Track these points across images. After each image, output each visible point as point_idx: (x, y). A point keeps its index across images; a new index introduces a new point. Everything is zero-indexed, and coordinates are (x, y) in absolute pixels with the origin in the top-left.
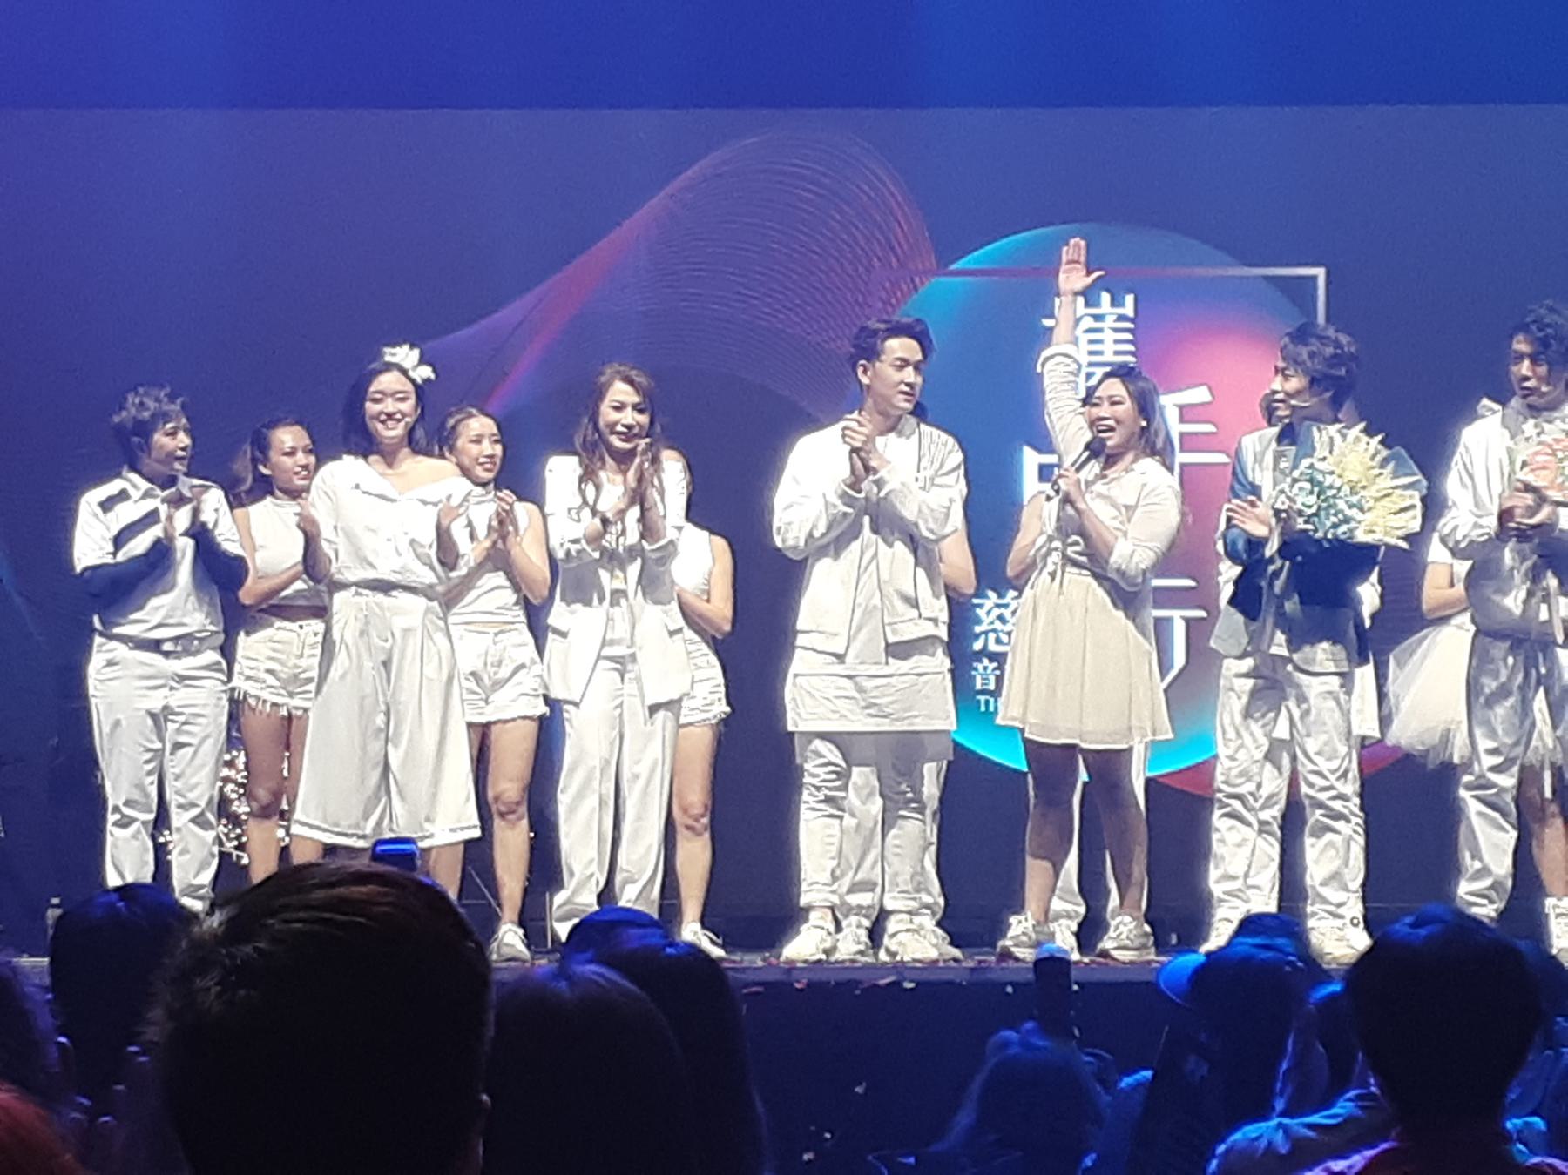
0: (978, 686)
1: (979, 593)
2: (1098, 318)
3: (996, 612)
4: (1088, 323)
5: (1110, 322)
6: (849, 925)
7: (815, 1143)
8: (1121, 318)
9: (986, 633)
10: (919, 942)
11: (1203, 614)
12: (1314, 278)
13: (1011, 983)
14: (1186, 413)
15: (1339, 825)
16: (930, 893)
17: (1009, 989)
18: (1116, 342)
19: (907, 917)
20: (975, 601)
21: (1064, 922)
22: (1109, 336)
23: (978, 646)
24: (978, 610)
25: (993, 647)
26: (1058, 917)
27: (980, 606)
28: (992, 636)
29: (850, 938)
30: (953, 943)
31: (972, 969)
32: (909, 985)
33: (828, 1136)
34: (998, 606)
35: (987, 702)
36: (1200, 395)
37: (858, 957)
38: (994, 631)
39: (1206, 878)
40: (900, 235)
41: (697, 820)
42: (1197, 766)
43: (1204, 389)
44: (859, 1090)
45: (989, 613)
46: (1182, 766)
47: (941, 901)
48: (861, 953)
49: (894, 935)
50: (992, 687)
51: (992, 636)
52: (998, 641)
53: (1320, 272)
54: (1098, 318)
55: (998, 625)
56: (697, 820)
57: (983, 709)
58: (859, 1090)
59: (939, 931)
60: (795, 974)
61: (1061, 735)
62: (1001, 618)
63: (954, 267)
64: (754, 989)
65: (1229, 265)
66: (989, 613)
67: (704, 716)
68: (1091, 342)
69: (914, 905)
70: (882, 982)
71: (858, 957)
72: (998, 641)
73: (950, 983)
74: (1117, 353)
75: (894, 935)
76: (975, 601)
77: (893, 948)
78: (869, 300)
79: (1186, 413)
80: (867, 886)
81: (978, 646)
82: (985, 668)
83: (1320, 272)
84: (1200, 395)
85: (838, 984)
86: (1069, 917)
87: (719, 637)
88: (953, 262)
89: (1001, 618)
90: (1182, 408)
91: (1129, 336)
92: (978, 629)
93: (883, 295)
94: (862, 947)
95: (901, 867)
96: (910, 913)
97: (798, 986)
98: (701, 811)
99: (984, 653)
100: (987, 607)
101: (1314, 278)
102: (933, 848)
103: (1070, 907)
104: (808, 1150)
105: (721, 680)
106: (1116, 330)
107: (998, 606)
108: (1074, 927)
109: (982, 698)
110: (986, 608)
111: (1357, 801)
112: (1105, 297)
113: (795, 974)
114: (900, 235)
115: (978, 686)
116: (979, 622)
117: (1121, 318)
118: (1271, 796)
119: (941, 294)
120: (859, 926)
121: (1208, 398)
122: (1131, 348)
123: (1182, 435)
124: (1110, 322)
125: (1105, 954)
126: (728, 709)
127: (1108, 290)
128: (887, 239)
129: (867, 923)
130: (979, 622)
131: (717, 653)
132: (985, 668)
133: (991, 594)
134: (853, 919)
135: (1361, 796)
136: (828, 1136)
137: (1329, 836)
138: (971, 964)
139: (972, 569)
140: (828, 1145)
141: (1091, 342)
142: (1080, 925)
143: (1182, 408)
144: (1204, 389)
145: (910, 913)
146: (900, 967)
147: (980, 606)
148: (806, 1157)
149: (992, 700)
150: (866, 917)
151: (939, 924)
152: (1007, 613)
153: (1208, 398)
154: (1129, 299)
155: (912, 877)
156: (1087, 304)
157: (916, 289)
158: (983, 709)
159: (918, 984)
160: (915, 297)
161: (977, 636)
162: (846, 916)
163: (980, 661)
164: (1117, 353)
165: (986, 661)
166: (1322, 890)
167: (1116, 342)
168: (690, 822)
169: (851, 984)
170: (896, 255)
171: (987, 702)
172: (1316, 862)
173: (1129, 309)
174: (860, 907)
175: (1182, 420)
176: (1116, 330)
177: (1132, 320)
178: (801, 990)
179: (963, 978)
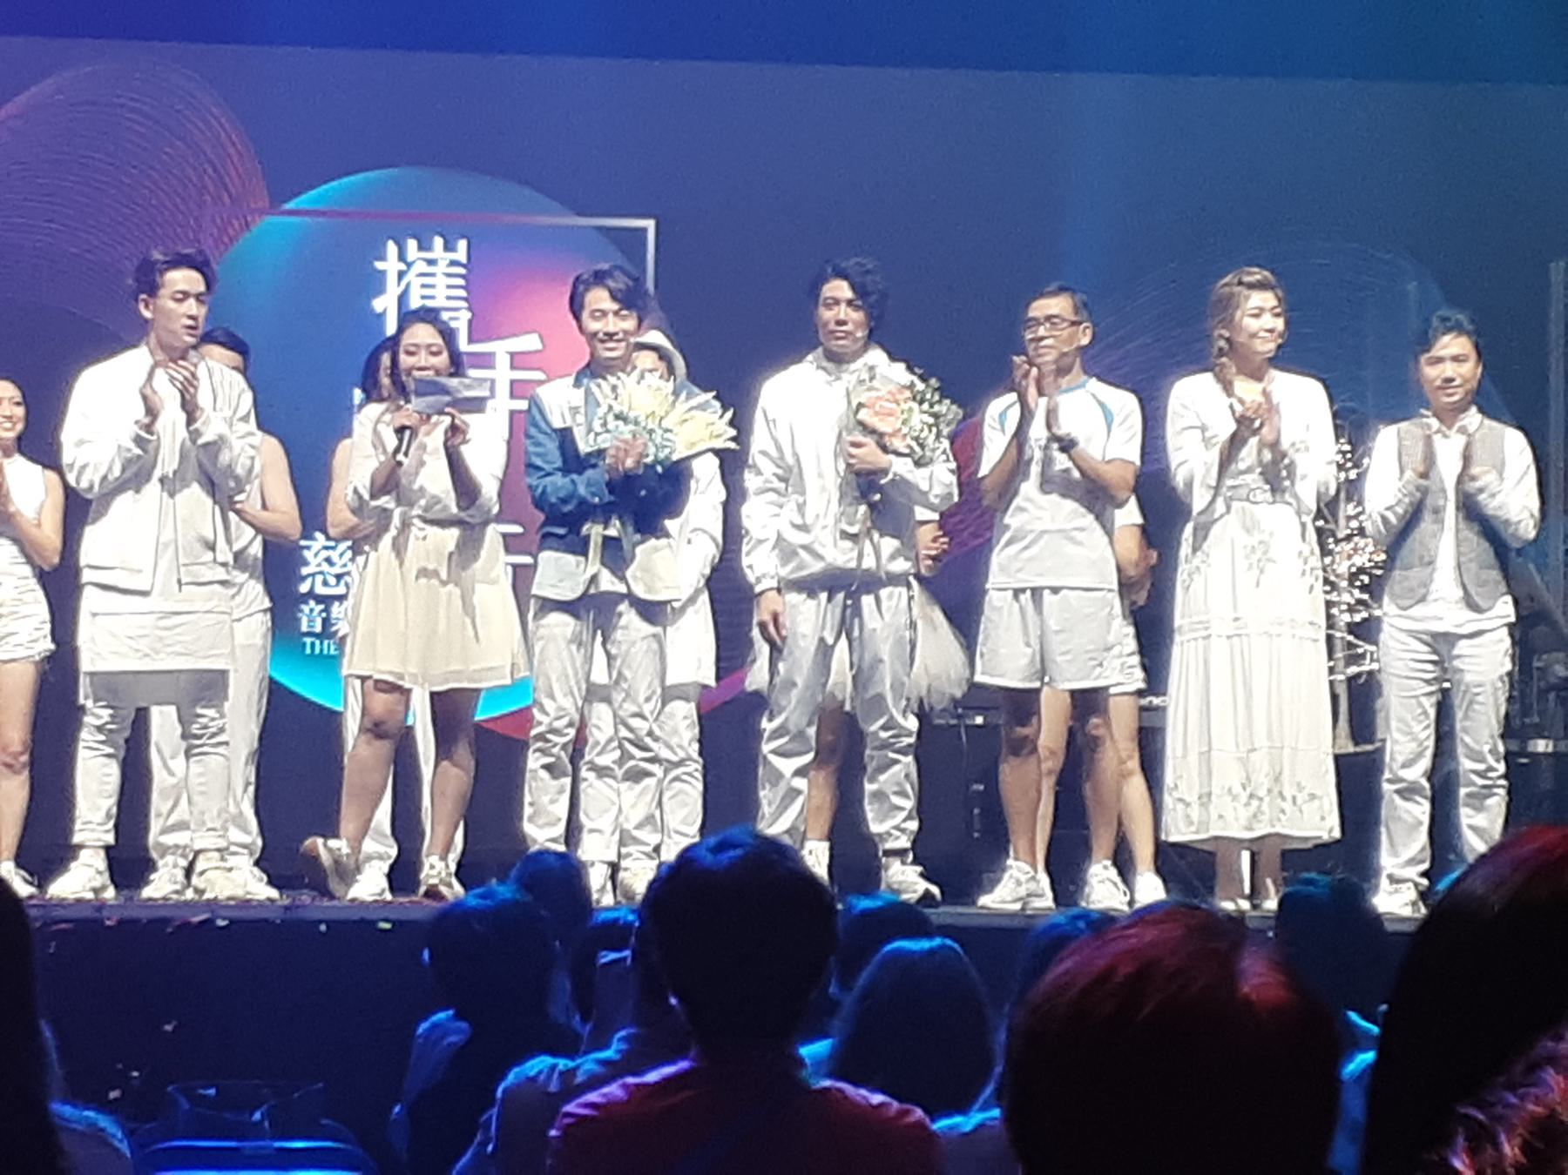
0: (304, 628)
1: (307, 534)
2: (431, 262)
3: (325, 554)
4: (421, 267)
5: (442, 267)
6: (166, 865)
7: (122, 1081)
8: (453, 263)
9: (313, 575)
10: (239, 881)
11: (528, 560)
12: (644, 230)
13: (327, 922)
14: (517, 360)
15: (654, 768)
16: (248, 833)
17: (323, 928)
18: (449, 287)
19: (216, 855)
20: (303, 543)
21: (374, 862)
22: (441, 281)
23: (304, 588)
24: (306, 553)
25: (320, 590)
26: (369, 858)
27: (308, 548)
28: (319, 579)
29: (167, 877)
30: (271, 883)
31: (287, 908)
32: (221, 923)
33: (135, 1074)
34: (326, 548)
35: (313, 645)
36: (530, 342)
37: (175, 896)
38: (321, 573)
39: (521, 818)
40: (233, 173)
41: (16, 758)
42: (521, 711)
43: (535, 337)
44: (168, 1028)
45: (316, 555)
46: (505, 711)
47: (259, 842)
48: (177, 892)
49: (202, 873)
50: (318, 629)
51: (319, 579)
52: (325, 583)
53: (650, 224)
54: (431, 262)
55: (325, 567)
56: (16, 758)
57: (308, 651)
58: (168, 1028)
59: (256, 870)
60: (105, 913)
61: (447, 681)
62: (328, 560)
63: (290, 206)
64: (63, 926)
65: (564, 215)
66: (316, 555)
67: (31, 652)
68: (423, 286)
69: (222, 843)
70: (196, 919)
71: (175, 896)
72: (325, 583)
73: (266, 921)
74: (449, 298)
75: (202, 873)
76: (303, 543)
77: (202, 886)
78: (201, 236)
79: (517, 360)
80: (182, 826)
81: (304, 588)
82: (312, 610)
83: (650, 224)
84: (530, 342)
85: (150, 921)
86: (381, 857)
87: (46, 568)
88: (289, 199)
89: (328, 560)
90: (513, 355)
91: (461, 282)
92: (305, 571)
93: (215, 231)
94: (178, 887)
95: (211, 808)
96: (218, 850)
97: (108, 923)
98: (17, 747)
99: (311, 594)
100: (315, 551)
101: (644, 230)
102: (252, 789)
103: (382, 849)
104: (114, 1089)
105: (46, 616)
106: (449, 275)
107: (326, 548)
108: (386, 870)
109: (308, 640)
110: (314, 550)
111: (696, 746)
112: (438, 242)
113: (105, 913)
114: (233, 173)
115: (304, 628)
116: (306, 563)
117: (453, 263)
118: (610, 740)
119: (274, 237)
120: (175, 866)
121: (539, 346)
122: (463, 293)
123: (513, 382)
124: (442, 267)
125: (432, 893)
126: (53, 647)
127: (442, 236)
128: (221, 177)
129: (184, 863)
130: (306, 563)
131: (44, 587)
132: (312, 610)
133: (318, 535)
134: (170, 859)
135: (700, 741)
136: (135, 1074)
137: (650, 782)
138: (286, 902)
139: (296, 513)
140: (134, 1082)
141: (423, 286)
142: (392, 867)
143: (513, 355)
144: (535, 337)
145: (218, 850)
146: (213, 904)
147: (308, 548)
148: (113, 1095)
149: (317, 642)
150: (184, 856)
151: (257, 863)
152: (334, 555)
153: (539, 346)
154: (462, 245)
155: (219, 815)
156: (421, 248)
157: (247, 225)
158: (308, 651)
159: (232, 922)
160: (247, 235)
161: (304, 578)
162: (162, 856)
163: (306, 603)
164: (449, 298)
165: (312, 603)
166: (636, 833)
167: (449, 287)
168: (9, 760)
169: (165, 921)
170: (227, 190)
171: (313, 645)
172: (634, 806)
173: (461, 254)
174: (177, 846)
175: (513, 367)
176: (449, 275)
177: (464, 266)
178: (109, 927)
179: (275, 916)
